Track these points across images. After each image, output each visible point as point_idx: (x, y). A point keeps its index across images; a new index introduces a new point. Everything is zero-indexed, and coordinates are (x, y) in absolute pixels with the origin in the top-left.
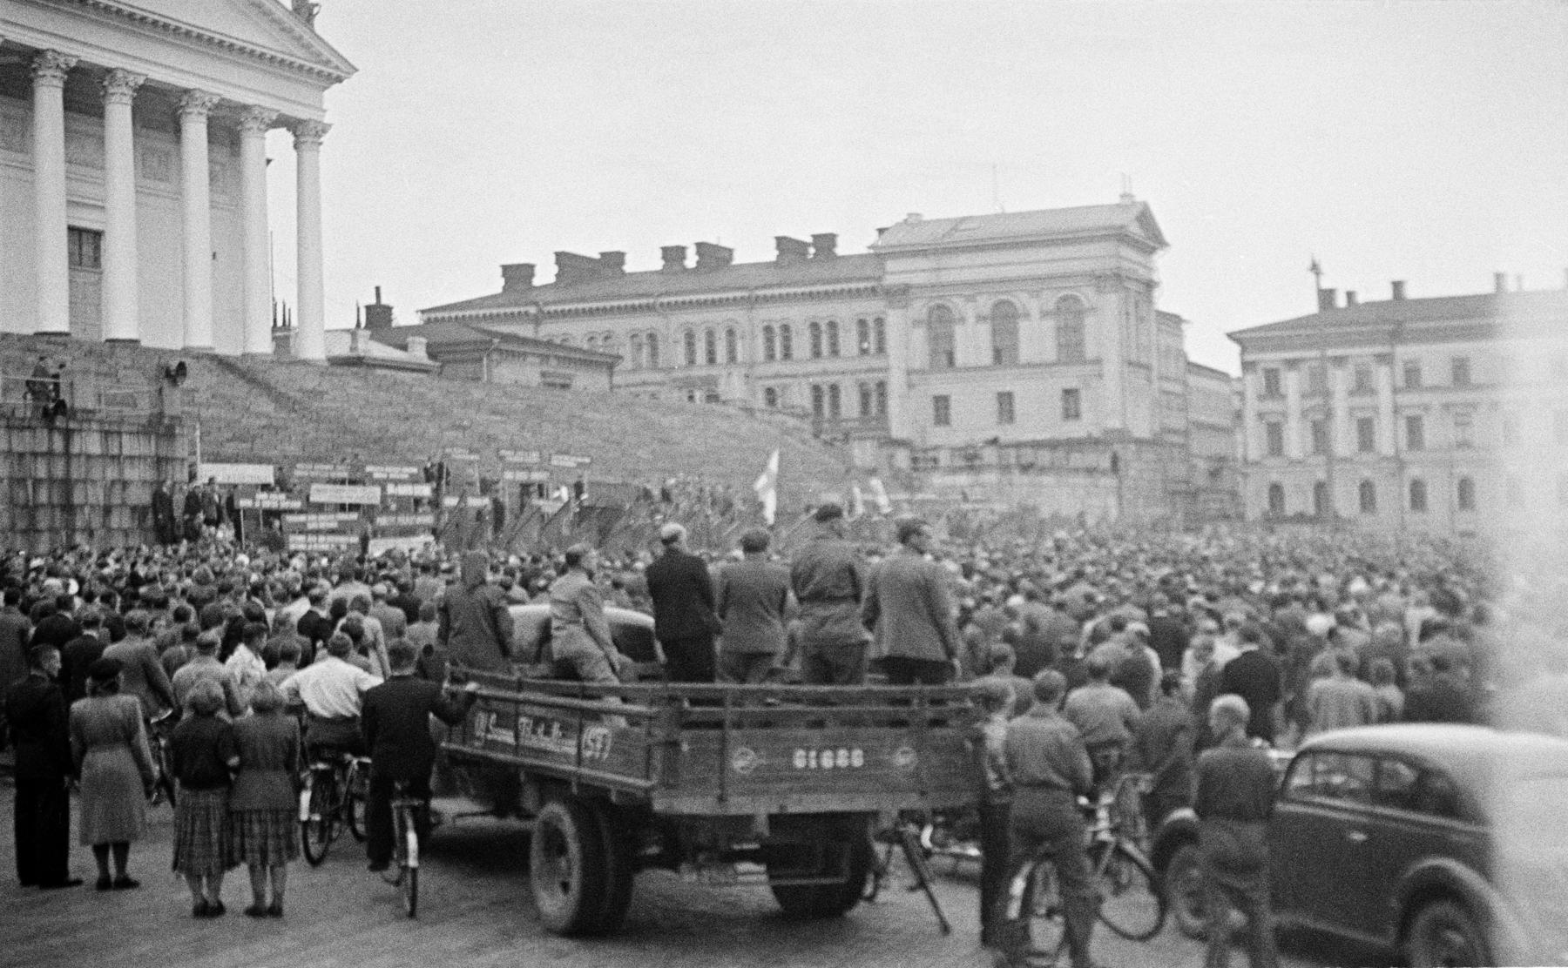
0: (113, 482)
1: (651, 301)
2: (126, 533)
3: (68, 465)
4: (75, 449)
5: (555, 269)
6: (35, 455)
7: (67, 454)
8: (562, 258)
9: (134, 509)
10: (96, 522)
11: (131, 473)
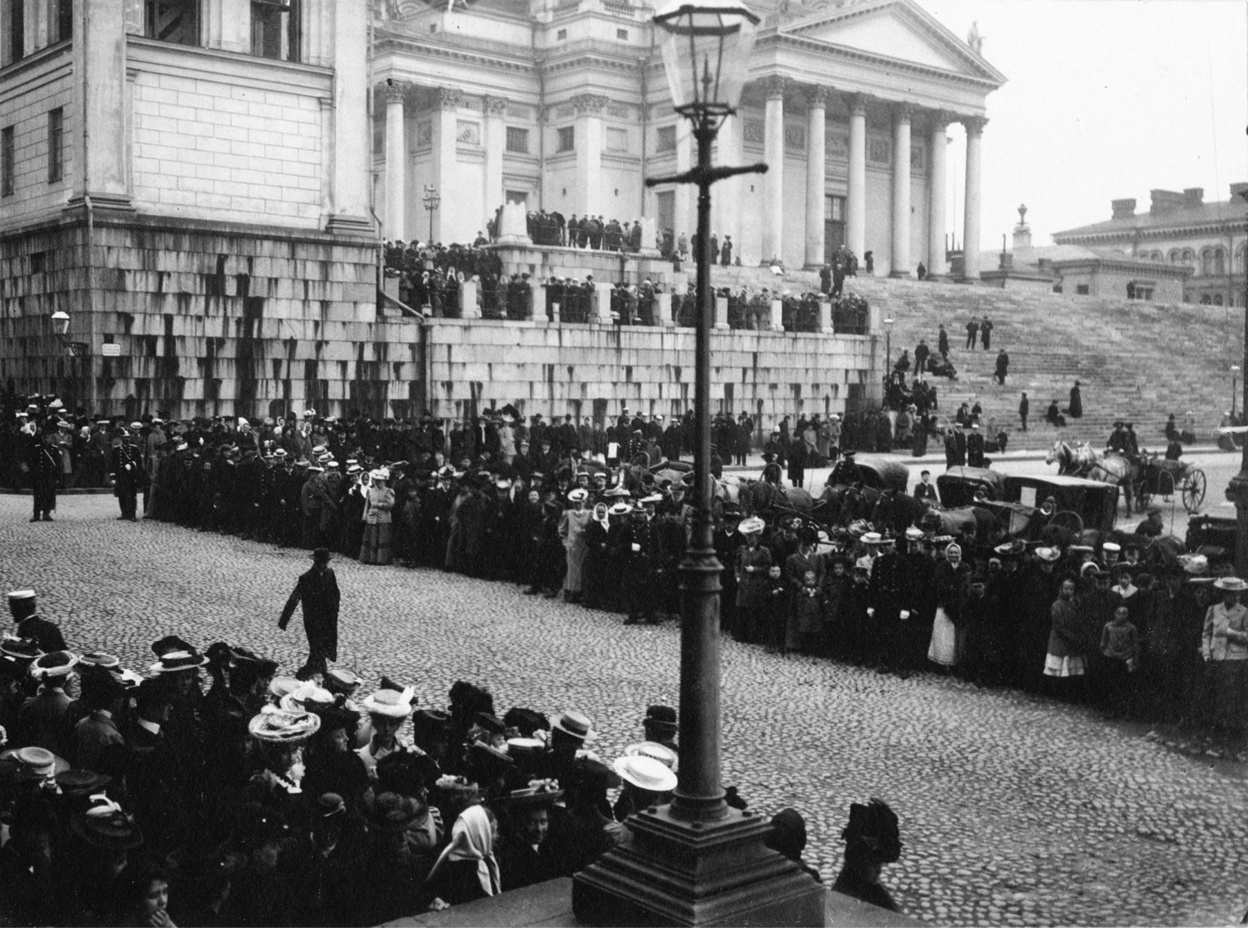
5: (1150, 202)
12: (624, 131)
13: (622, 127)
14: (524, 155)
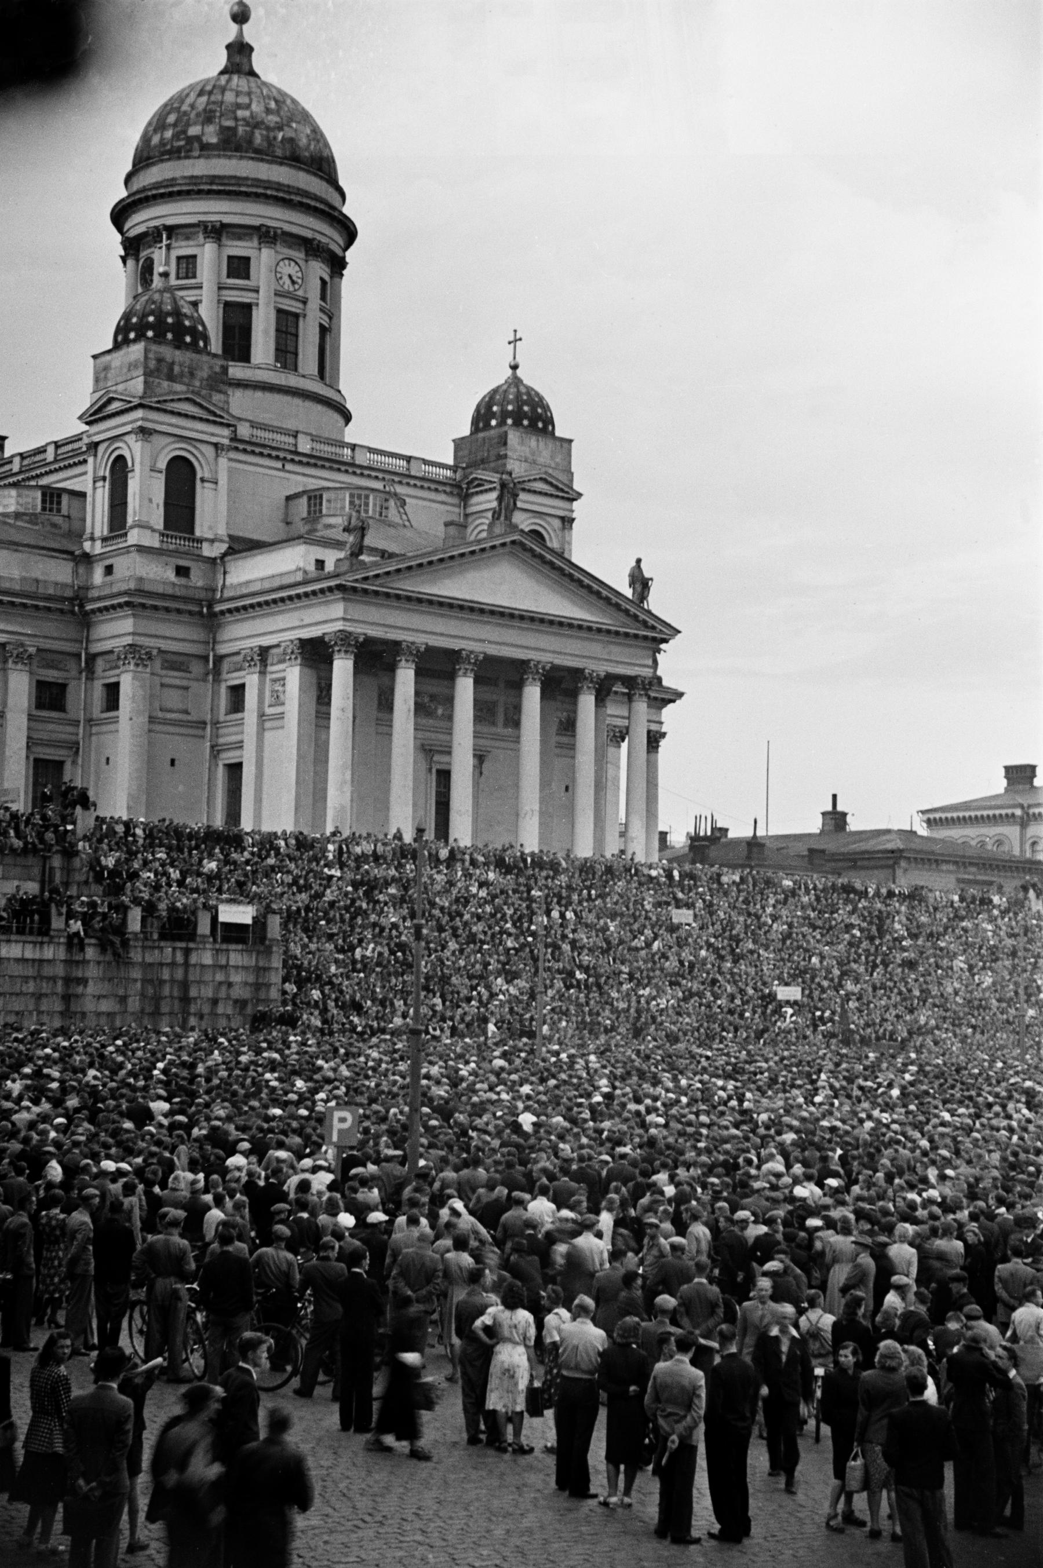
0: (220, 983)
2: (228, 1017)
3: (186, 972)
4: (193, 959)
6: (161, 965)
7: (186, 964)
9: (236, 1001)
10: (206, 1009)
11: (236, 978)
12: (186, 688)
13: (185, 683)
14: (62, 715)
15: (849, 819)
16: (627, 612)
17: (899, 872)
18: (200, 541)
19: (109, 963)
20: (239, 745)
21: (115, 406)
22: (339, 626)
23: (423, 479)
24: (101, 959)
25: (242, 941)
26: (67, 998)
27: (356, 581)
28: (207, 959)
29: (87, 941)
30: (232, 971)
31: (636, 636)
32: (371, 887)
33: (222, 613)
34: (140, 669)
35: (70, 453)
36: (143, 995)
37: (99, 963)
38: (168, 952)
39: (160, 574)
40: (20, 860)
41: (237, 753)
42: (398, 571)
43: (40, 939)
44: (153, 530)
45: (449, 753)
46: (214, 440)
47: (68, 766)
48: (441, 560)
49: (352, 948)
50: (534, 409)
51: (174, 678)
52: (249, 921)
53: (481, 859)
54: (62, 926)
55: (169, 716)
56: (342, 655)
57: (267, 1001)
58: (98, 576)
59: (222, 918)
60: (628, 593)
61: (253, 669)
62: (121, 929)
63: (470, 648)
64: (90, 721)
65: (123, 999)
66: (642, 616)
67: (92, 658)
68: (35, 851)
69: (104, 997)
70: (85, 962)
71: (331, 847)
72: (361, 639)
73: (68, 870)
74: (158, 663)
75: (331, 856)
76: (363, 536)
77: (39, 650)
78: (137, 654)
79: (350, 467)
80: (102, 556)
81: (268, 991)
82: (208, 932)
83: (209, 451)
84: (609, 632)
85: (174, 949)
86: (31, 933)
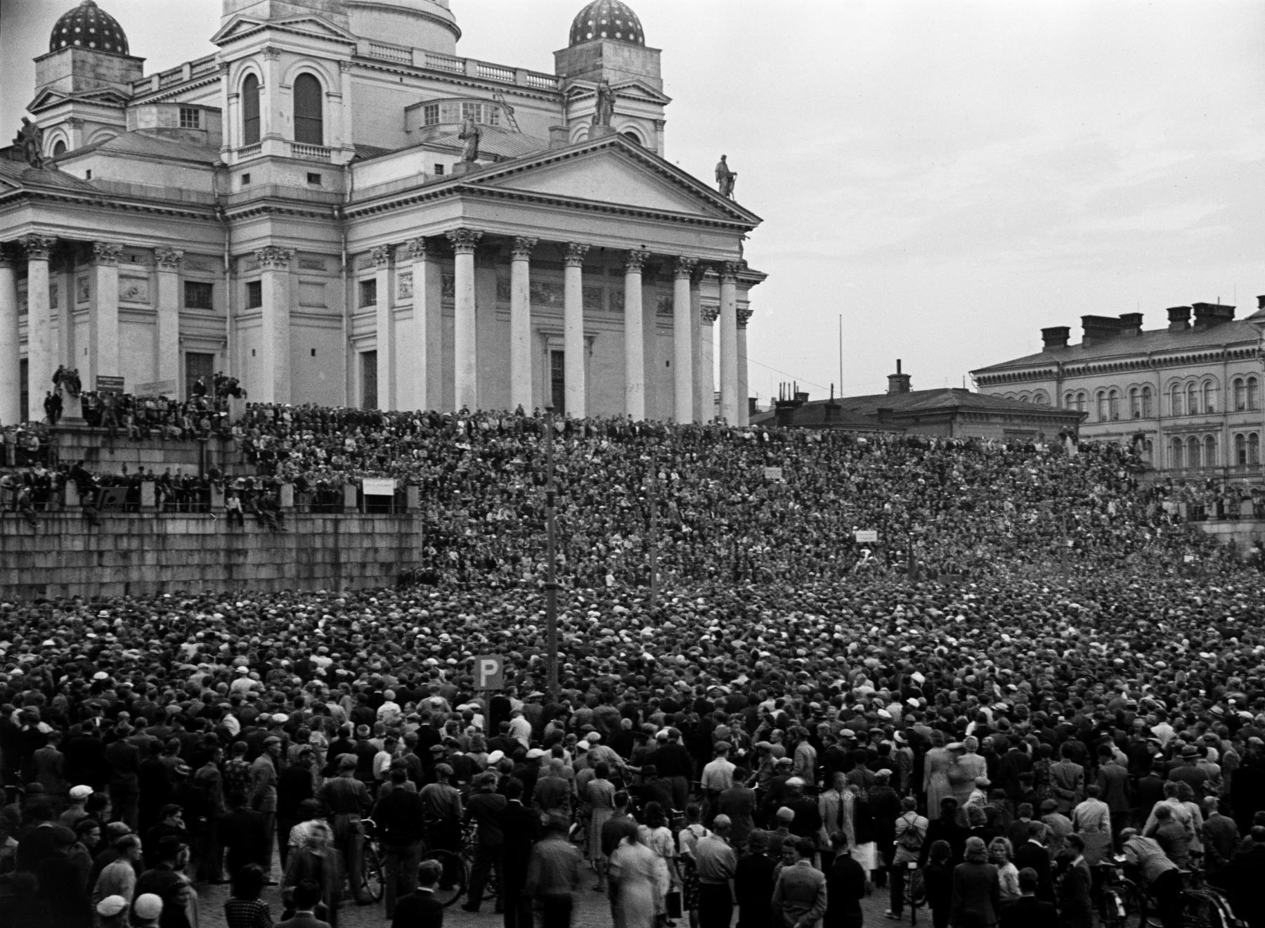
0: (368, 549)
1: (1145, 359)
3: (336, 541)
5: (1082, 332)
6: (314, 534)
7: (336, 533)
8: (1089, 322)
9: (382, 564)
10: (356, 572)
11: (382, 544)
12: (322, 285)
13: (319, 280)
15: (912, 381)
16: (715, 204)
17: (956, 427)
18: (329, 150)
19: (266, 535)
20: (373, 335)
21: (244, 29)
22: (459, 224)
23: (528, 89)
24: (258, 531)
25: (384, 510)
26: (229, 567)
27: (473, 183)
28: (355, 527)
29: (245, 516)
30: (377, 538)
31: (724, 225)
32: (498, 458)
33: (352, 215)
34: (280, 268)
35: (203, 72)
36: (298, 562)
37: (257, 535)
38: (320, 523)
39: (293, 181)
40: (181, 446)
41: (371, 342)
42: (510, 172)
43: (201, 516)
44: (285, 142)
45: (562, 336)
46: (338, 57)
47: (217, 360)
48: (548, 162)
49: (484, 514)
50: (625, 22)
51: (311, 275)
52: (391, 493)
53: (594, 429)
54: (222, 503)
55: (307, 310)
56: (463, 250)
57: (410, 562)
58: (236, 184)
59: (366, 491)
60: (716, 186)
61: (383, 266)
62: (275, 505)
63: (578, 241)
64: (235, 317)
65: (280, 567)
66: (729, 208)
67: (235, 259)
68: (193, 436)
69: (263, 565)
70: (244, 535)
71: (461, 423)
72: (479, 236)
73: (223, 453)
74: (295, 262)
75: (461, 431)
76: (477, 142)
77: (186, 253)
78: (275, 254)
79: (461, 79)
80: (240, 166)
81: (411, 555)
82: (354, 504)
83: (333, 68)
84: (699, 222)
85: (325, 520)
86: (194, 511)
